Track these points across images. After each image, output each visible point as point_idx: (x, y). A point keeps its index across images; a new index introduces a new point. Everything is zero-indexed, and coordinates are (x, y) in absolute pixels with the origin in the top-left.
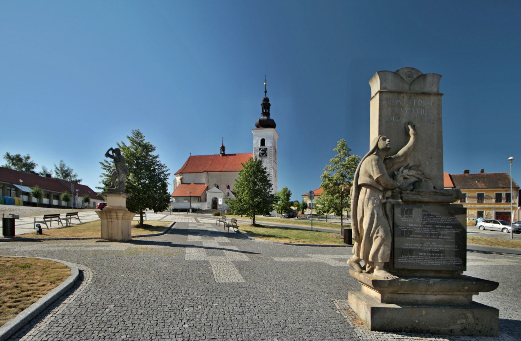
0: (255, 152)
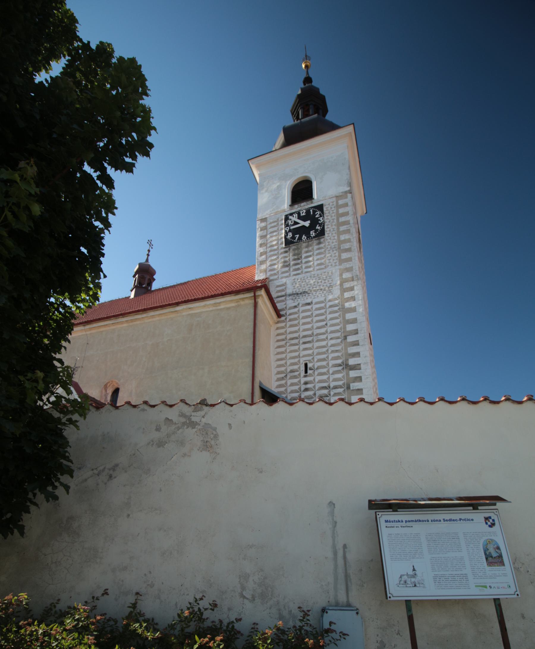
0: (262, 237)
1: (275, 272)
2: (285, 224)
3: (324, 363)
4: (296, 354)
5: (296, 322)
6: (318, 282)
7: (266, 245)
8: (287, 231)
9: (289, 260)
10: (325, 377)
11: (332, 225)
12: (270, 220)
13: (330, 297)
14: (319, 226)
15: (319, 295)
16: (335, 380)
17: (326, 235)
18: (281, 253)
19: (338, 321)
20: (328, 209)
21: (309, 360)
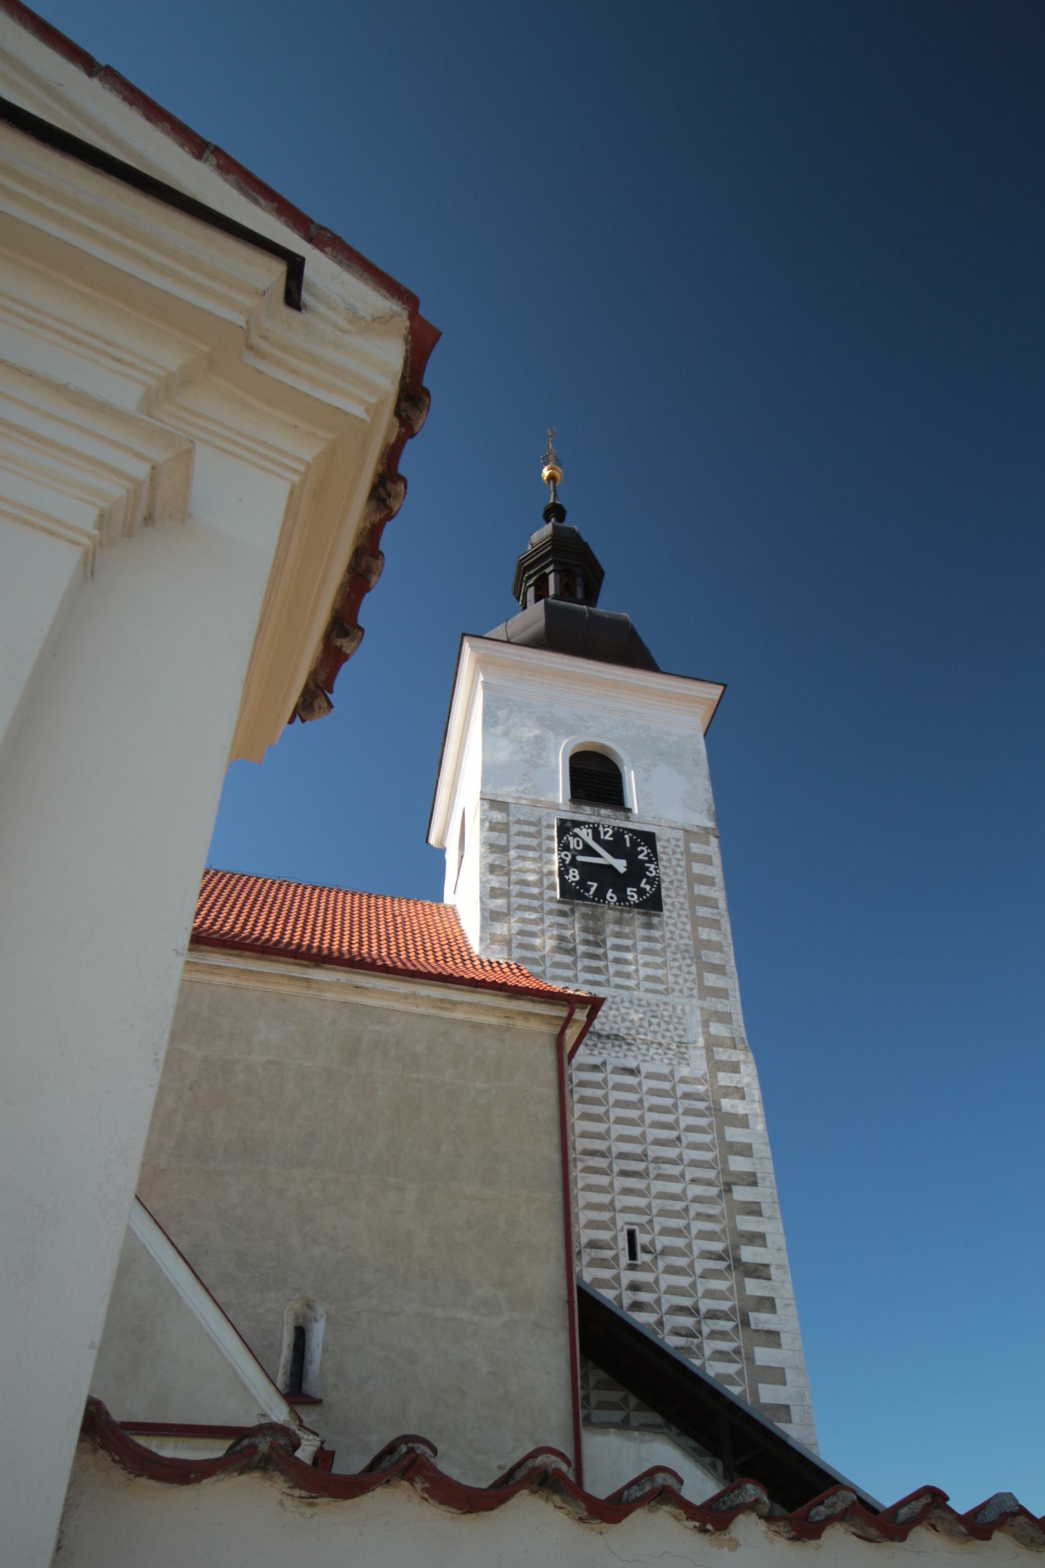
1: (536, 955)
2: (559, 842)
3: (680, 1242)
4: (604, 1198)
5: (599, 1110)
6: (650, 1024)
7: (508, 874)
8: (567, 862)
9: (573, 936)
10: (684, 1281)
11: (677, 895)
12: (515, 814)
13: (684, 1071)
14: (645, 884)
15: (656, 1057)
16: (710, 1294)
17: (666, 913)
18: (551, 912)
19: (706, 1138)
20: (666, 850)
21: (641, 1225)
